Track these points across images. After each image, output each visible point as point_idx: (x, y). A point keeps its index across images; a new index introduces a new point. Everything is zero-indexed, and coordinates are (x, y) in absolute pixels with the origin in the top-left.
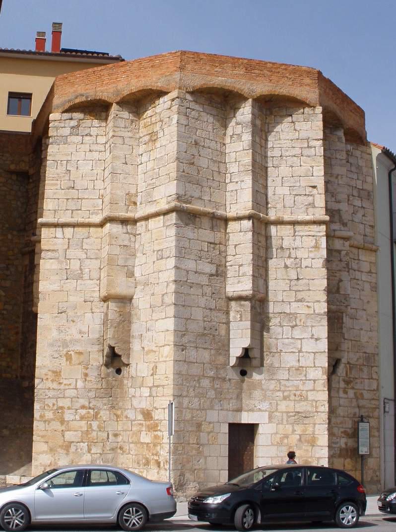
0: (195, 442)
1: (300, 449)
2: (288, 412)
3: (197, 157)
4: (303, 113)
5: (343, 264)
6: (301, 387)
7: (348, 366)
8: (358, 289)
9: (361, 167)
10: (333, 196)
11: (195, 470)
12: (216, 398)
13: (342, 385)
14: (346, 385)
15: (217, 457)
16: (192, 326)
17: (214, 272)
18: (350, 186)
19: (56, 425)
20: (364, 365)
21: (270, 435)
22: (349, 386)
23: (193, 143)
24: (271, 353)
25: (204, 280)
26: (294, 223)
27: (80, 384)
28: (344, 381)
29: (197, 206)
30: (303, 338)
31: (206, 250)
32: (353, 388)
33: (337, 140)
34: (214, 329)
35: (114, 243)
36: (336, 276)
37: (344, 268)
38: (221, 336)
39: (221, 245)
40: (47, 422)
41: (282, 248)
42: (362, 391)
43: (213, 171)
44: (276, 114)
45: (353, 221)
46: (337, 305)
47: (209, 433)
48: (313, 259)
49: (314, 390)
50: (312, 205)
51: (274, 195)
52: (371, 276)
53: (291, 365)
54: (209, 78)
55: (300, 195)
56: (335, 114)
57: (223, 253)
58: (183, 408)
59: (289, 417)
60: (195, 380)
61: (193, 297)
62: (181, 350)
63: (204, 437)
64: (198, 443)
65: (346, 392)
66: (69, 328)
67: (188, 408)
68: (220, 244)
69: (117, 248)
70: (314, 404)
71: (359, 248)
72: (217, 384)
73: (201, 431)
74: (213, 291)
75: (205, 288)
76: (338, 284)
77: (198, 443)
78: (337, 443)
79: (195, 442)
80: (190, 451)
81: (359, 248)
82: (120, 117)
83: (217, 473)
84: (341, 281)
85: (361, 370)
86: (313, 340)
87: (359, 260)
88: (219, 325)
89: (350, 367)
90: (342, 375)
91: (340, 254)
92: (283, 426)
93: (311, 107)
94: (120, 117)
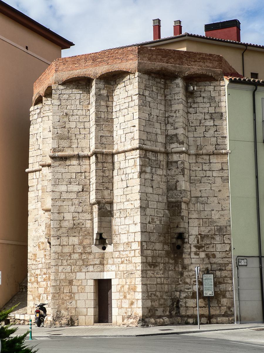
0: (68, 292)
1: (129, 294)
2: (123, 271)
3: (67, 123)
4: (130, 79)
5: (179, 170)
6: (129, 255)
7: (199, 236)
8: (209, 183)
9: (214, 97)
10: (172, 126)
11: (68, 308)
12: (83, 265)
13: (194, 249)
14: (197, 250)
15: (85, 300)
16: (65, 224)
17: (81, 190)
18: (202, 113)
19: (35, 285)
20: (215, 234)
21: (116, 286)
22: (201, 249)
23: (64, 114)
24: (116, 234)
25: (74, 196)
26: (124, 152)
27: (43, 260)
28: (195, 246)
29: (68, 152)
30: (130, 224)
31: (75, 177)
32: (204, 251)
33: (175, 86)
34: (81, 224)
35: (44, 179)
36: (174, 179)
37: (180, 172)
38: (87, 228)
39: (86, 173)
40: (32, 283)
41: (120, 168)
42: (214, 253)
43: (79, 129)
44: (117, 83)
45: (204, 137)
46: (175, 198)
47: (78, 286)
48: (133, 173)
49: (135, 256)
50: (133, 139)
51: (117, 136)
52: (222, 172)
53: (125, 241)
54: (71, 72)
55: (128, 133)
56: (109, 84)
57: (88, 178)
58: (58, 272)
59: (124, 274)
60: (67, 255)
61: (65, 207)
62: (56, 239)
63: (75, 289)
64: (70, 292)
65: (196, 254)
66: (39, 229)
67: (62, 272)
68: (85, 172)
69: (46, 182)
70: (135, 265)
71: (210, 155)
72: (84, 257)
73: (72, 285)
74: (80, 201)
75: (74, 201)
76: (176, 184)
77: (70, 292)
78: (190, 288)
79: (68, 292)
80: (64, 297)
81: (210, 155)
82: (47, 105)
83: (85, 310)
84: (177, 181)
85: (213, 238)
86: (134, 225)
87: (210, 163)
88: (85, 221)
89: (201, 237)
90: (193, 243)
91: (177, 163)
92: (122, 279)
93: (133, 74)
94: (47, 105)
